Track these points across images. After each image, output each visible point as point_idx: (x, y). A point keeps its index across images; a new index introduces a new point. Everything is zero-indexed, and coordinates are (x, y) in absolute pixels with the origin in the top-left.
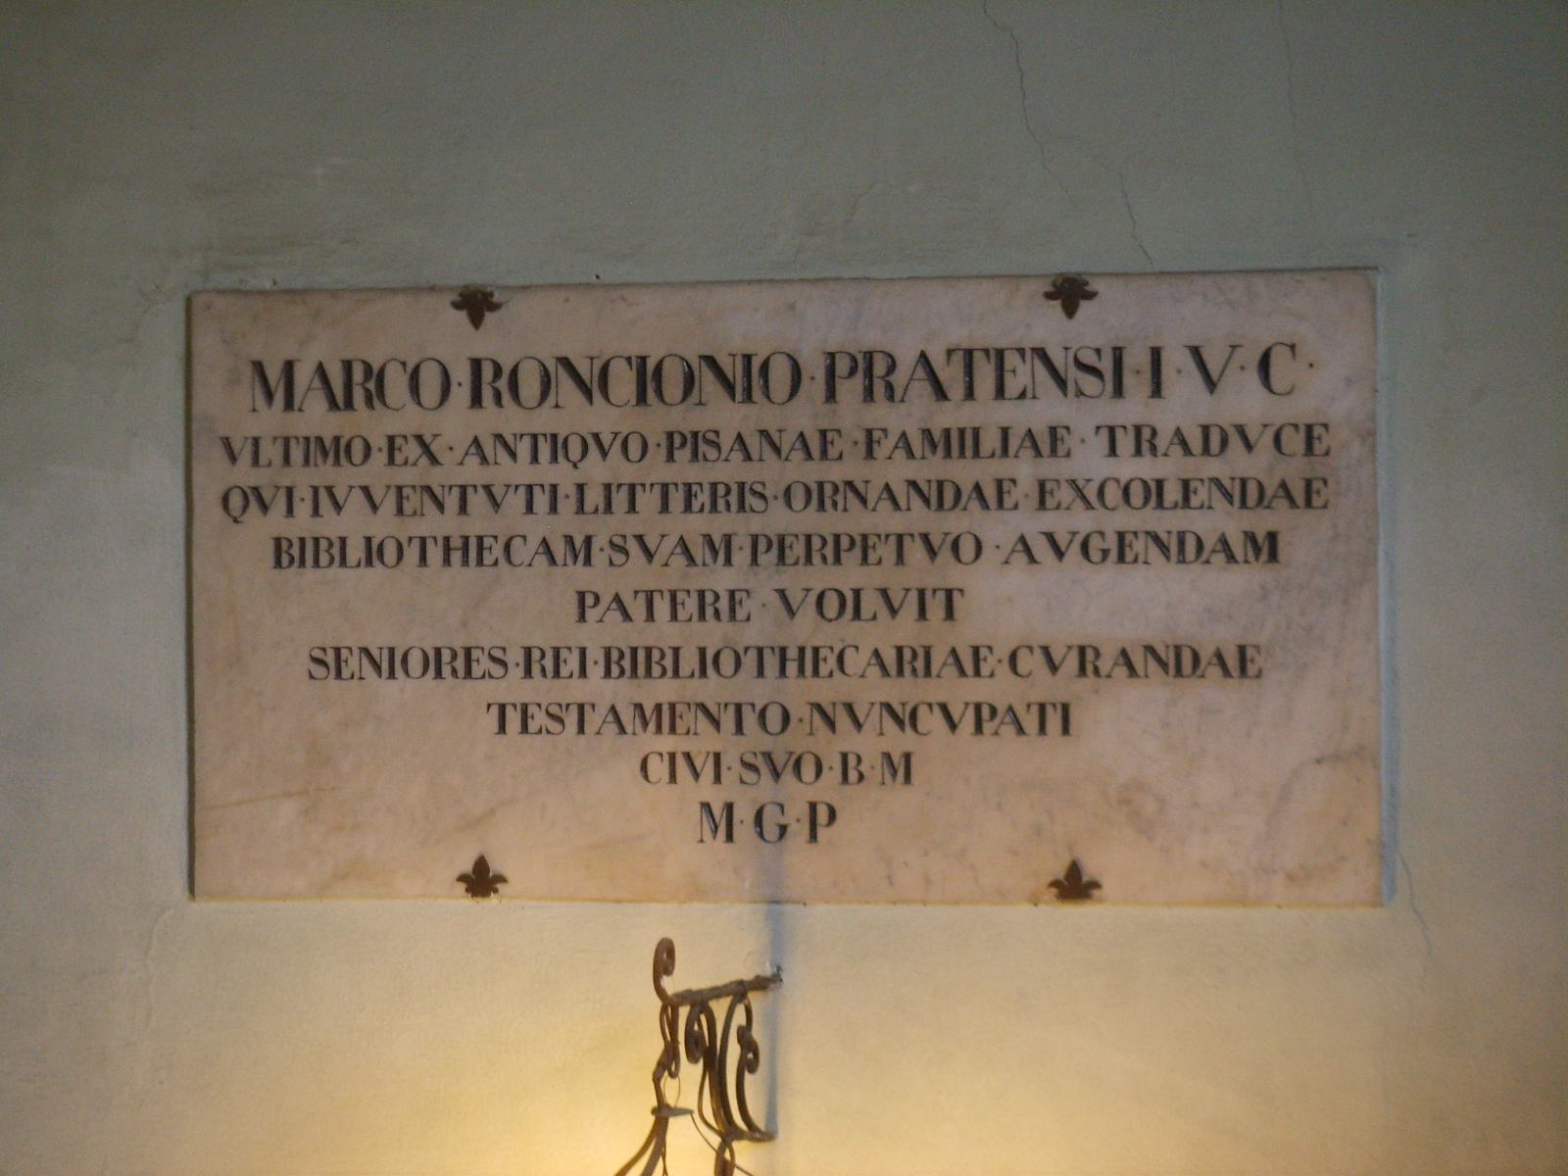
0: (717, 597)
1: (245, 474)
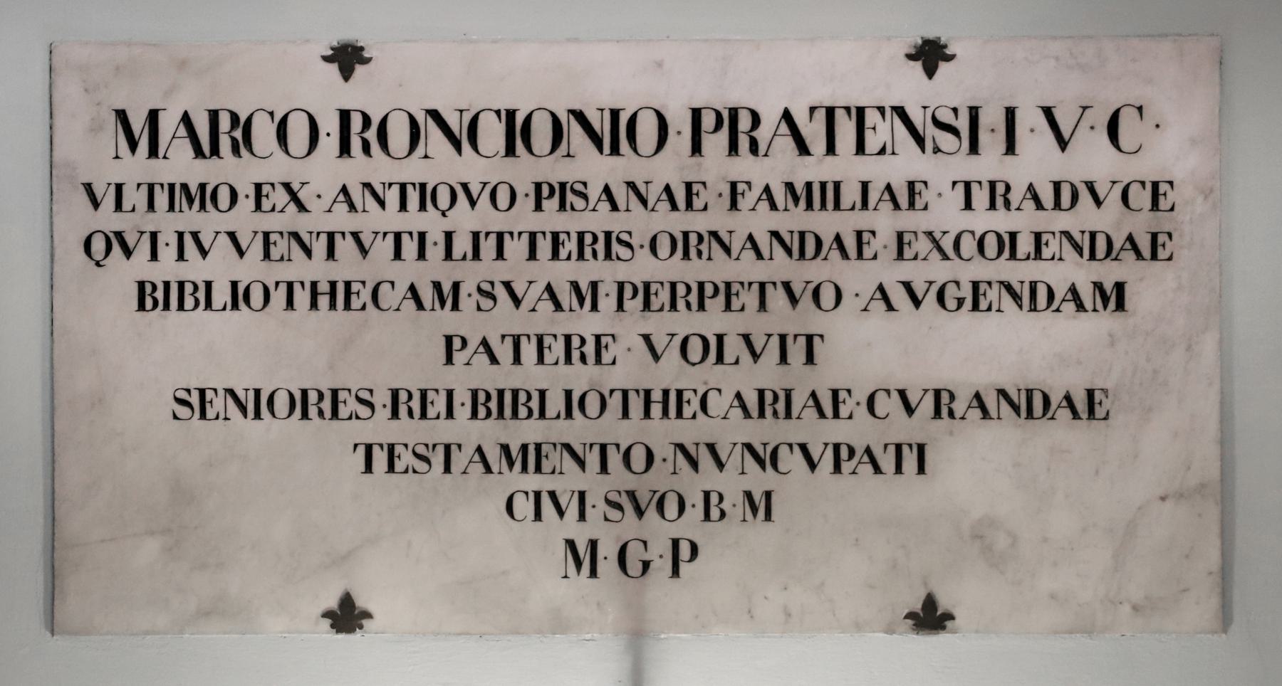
0: (583, 341)
1: (108, 219)
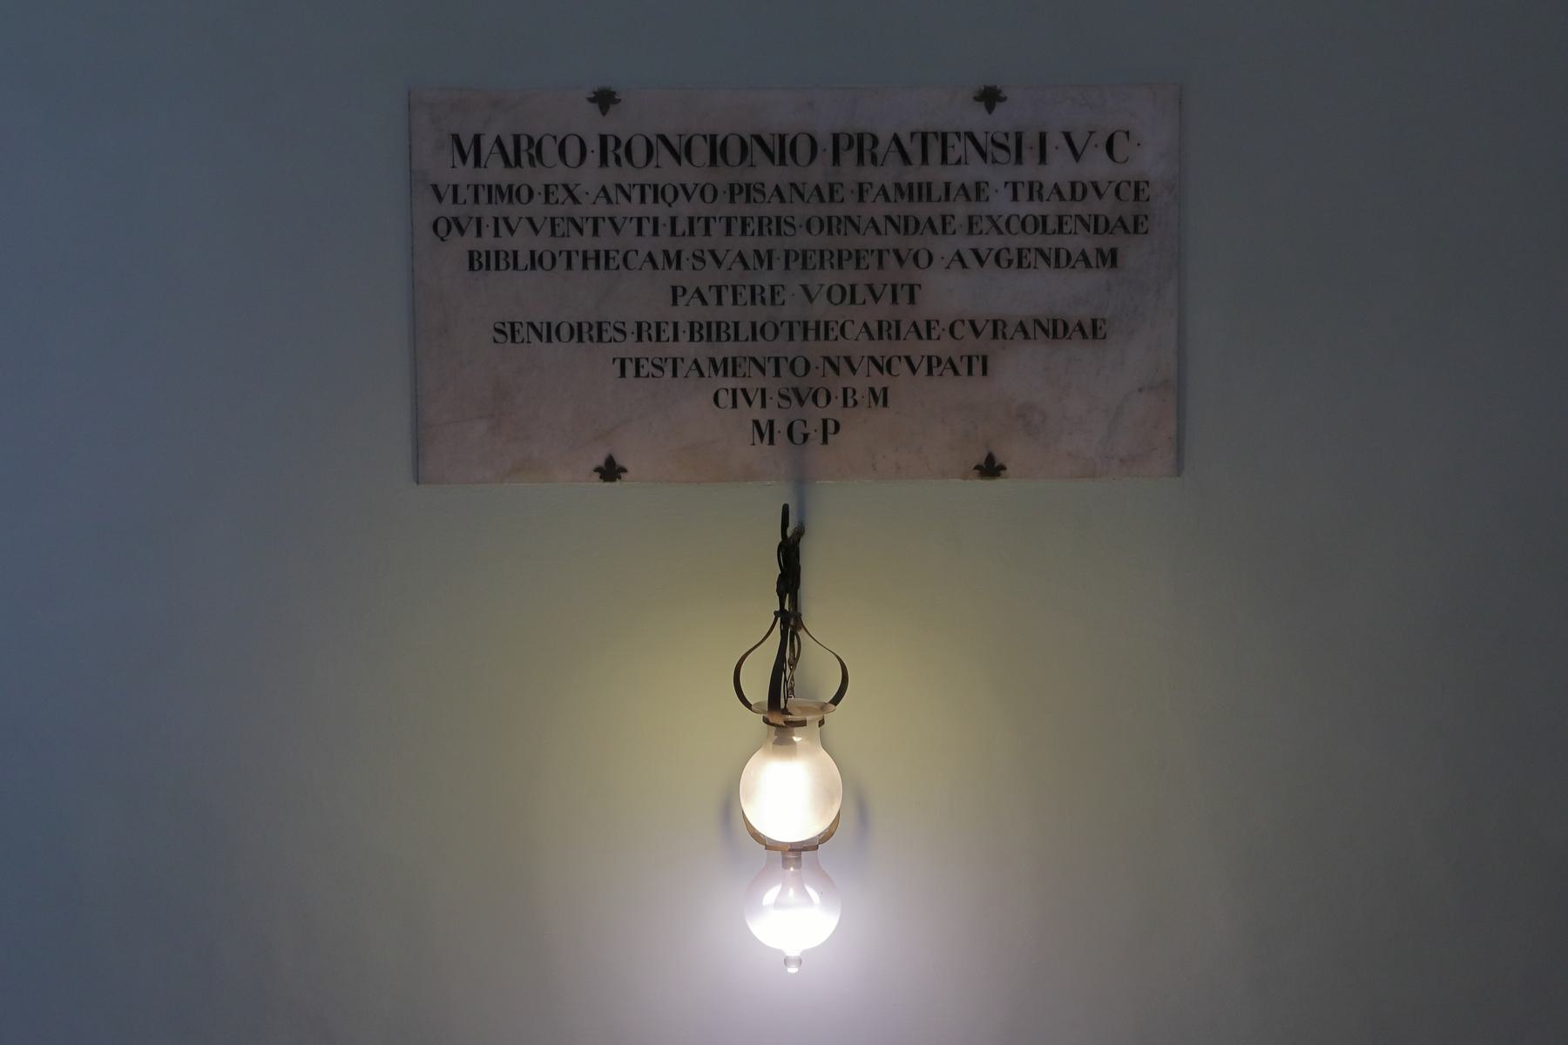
1: (448, 209)
